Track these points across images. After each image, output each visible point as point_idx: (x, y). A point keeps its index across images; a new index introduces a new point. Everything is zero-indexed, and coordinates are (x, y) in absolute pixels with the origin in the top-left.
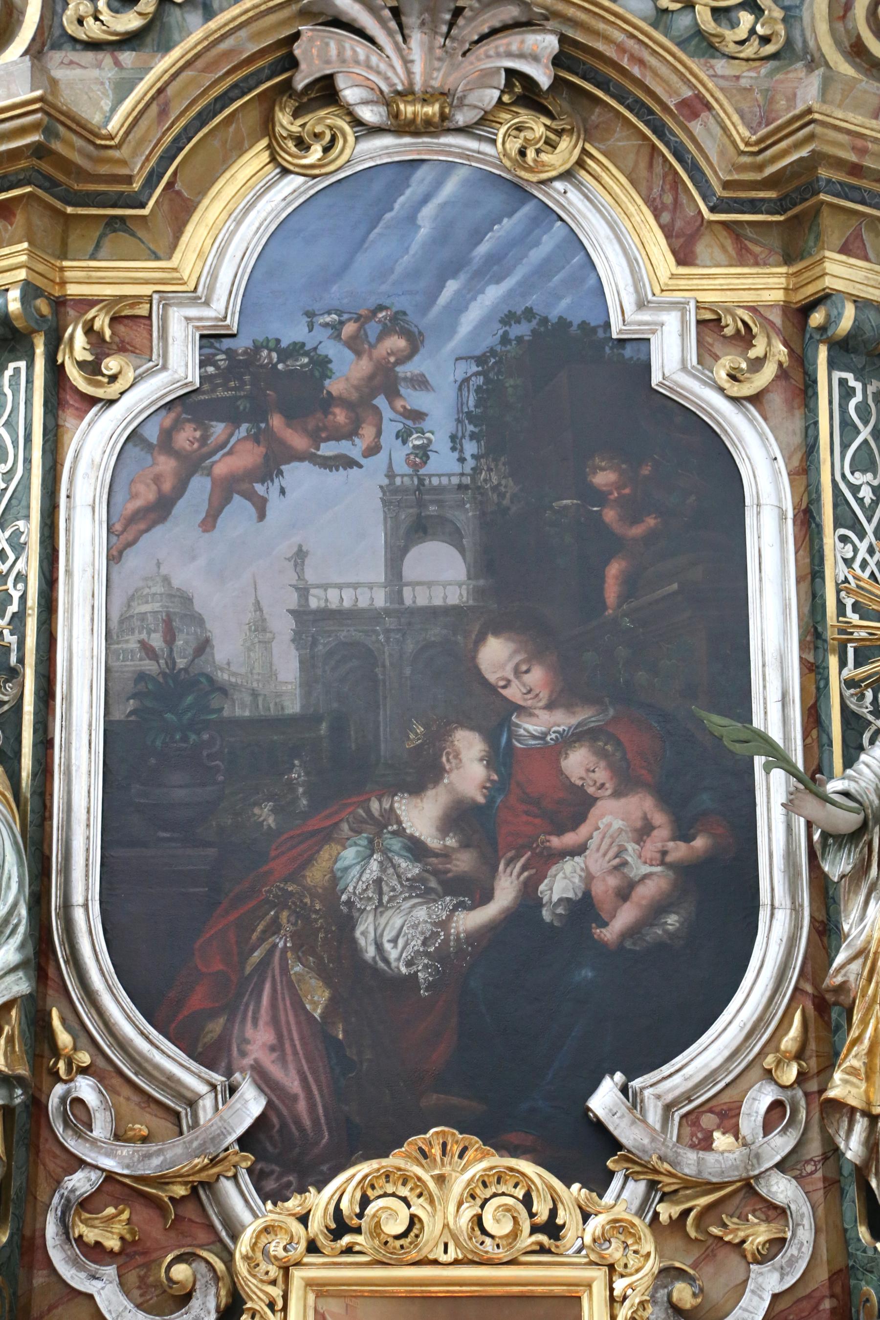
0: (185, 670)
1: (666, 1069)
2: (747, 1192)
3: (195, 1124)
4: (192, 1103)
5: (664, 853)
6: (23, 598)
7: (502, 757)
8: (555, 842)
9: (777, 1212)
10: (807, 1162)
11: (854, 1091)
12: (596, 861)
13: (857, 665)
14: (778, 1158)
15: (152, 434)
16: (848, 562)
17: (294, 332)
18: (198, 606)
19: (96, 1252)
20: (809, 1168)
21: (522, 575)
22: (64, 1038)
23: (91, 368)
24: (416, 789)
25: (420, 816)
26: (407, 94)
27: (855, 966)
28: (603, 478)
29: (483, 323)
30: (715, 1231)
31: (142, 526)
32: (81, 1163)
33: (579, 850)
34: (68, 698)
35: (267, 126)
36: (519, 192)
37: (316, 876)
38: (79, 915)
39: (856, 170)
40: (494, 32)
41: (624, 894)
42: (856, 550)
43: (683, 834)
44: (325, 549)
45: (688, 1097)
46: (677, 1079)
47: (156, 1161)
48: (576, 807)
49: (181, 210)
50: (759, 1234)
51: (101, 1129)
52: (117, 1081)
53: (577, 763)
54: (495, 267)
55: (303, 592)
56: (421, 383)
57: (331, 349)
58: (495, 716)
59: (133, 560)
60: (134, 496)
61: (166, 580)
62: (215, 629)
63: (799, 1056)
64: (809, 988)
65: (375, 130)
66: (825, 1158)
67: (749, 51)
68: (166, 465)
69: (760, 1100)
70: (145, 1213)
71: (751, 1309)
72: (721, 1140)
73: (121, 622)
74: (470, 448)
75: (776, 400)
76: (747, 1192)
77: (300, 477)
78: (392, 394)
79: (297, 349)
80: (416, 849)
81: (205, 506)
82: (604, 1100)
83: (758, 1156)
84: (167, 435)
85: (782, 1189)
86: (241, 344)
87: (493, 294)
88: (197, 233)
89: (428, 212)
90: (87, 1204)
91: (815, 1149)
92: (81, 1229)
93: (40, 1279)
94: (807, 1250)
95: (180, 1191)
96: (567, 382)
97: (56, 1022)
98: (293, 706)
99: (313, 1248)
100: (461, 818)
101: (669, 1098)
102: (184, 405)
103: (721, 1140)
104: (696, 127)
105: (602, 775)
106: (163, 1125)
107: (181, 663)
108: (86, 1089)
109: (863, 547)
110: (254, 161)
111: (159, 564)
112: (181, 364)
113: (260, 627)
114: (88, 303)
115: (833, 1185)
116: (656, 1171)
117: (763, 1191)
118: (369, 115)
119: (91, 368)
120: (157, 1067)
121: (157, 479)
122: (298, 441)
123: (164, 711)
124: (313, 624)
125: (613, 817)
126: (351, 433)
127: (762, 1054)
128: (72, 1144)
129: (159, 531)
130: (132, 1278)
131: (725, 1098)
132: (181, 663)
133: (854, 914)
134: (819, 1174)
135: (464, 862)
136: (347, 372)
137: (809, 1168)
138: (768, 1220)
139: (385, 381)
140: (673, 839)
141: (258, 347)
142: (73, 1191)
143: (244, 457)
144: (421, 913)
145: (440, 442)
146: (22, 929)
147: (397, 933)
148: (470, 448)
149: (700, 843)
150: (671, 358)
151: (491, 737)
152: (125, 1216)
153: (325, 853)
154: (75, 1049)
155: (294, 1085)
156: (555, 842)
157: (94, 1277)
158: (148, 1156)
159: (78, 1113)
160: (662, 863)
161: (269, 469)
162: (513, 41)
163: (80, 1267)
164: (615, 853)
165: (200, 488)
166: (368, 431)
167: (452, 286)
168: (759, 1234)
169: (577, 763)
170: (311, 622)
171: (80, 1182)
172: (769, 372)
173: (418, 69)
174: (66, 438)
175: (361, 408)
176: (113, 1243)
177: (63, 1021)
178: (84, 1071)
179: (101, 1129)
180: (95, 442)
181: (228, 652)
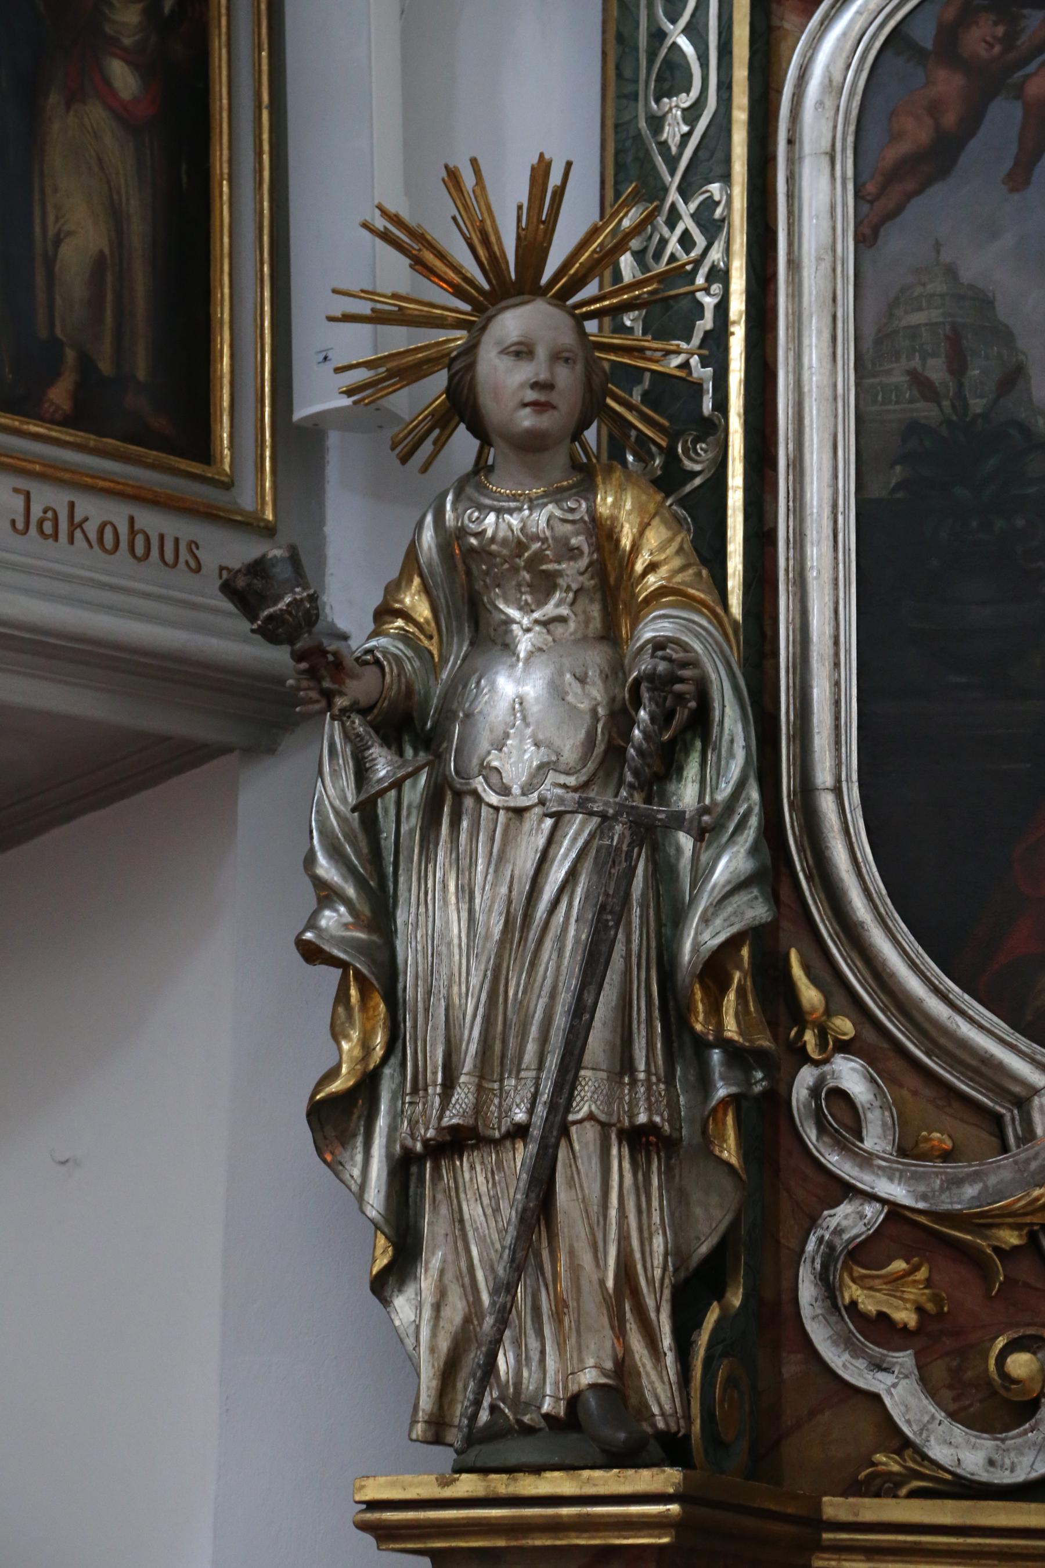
0: (985, 416)
3: (1028, 1135)
6: (722, 308)
15: (925, 35)
18: (1002, 312)
19: (879, 1330)
22: (810, 995)
31: (910, 185)
32: (847, 1191)
34: (797, 465)
38: (827, 804)
47: (970, 1191)
51: (875, 1139)
52: (896, 1065)
59: (896, 242)
60: (895, 137)
61: (951, 272)
68: (948, 84)
73: (878, 342)
81: (1014, 149)
90: (863, 1254)
92: (853, 1292)
93: (792, 1367)
95: (1012, 1238)
97: (797, 971)
106: (976, 1136)
107: (977, 405)
108: (850, 1075)
111: (937, 247)
120: (964, 1044)
121: (934, 109)
128: (833, 1160)
129: (937, 192)
130: (939, 1370)
132: (977, 405)
142: (838, 1231)
146: (754, 821)
152: (922, 1274)
154: (828, 1013)
157: (878, 1366)
158: (958, 1182)
159: (839, 1113)
163: (856, 1352)
165: (1004, 118)
171: (849, 1220)
174: (784, 47)
176: (905, 1316)
177: (807, 968)
178: (844, 1047)
179: (875, 1139)
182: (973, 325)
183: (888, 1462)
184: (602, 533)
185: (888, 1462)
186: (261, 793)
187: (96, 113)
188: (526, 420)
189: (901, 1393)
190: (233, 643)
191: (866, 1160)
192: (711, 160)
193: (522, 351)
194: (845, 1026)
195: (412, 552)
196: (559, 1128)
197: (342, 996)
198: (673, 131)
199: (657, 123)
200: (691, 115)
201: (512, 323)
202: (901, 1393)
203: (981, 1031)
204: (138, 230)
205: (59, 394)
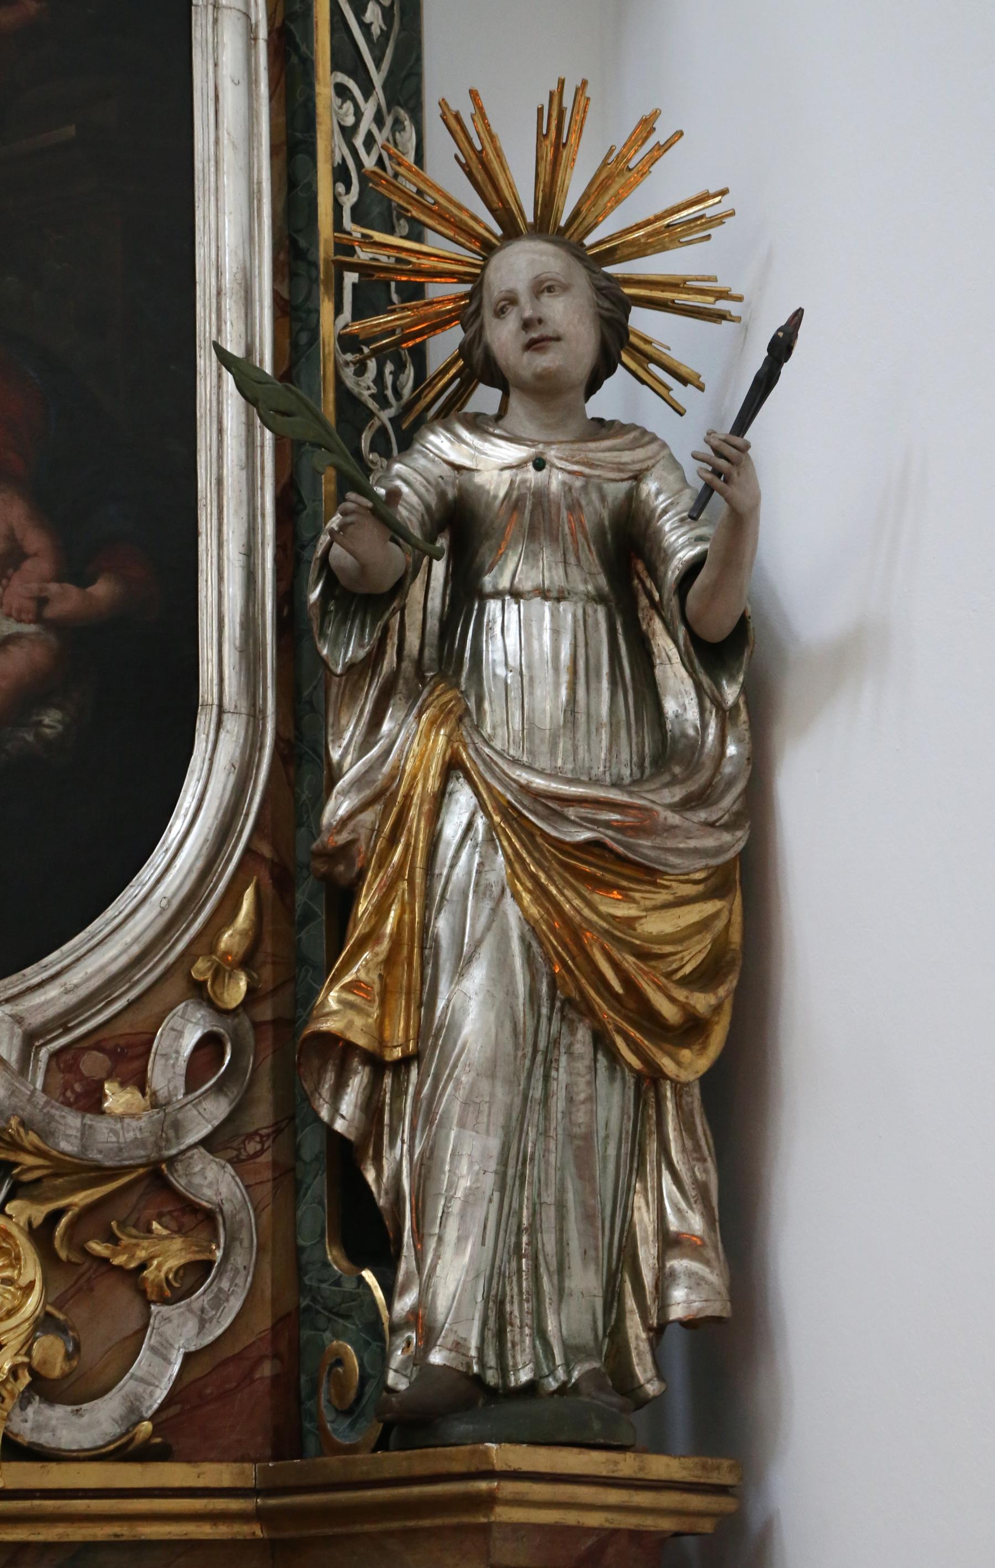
1: (33, 974)
2: (155, 1184)
5: (42, 601)
9: (198, 1218)
10: (250, 1137)
11: (359, 1021)
13: (357, 316)
14: (205, 1130)
16: (348, 133)
20: (252, 1147)
27: (368, 817)
30: (97, 1247)
42: (358, 114)
43: (75, 571)
45: (63, 1022)
46: (52, 992)
63: (247, 962)
64: (265, 850)
66: (277, 1131)
69: (186, 1032)
71: (150, 1378)
72: (117, 1098)
76: (155, 1184)
83: (177, 1126)
85: (214, 1182)
91: (262, 1115)
94: (244, 1283)
101: (35, 1020)
103: (117, 1098)
109: (369, 110)
115: (288, 1178)
116: (16, 1146)
117: (179, 1183)
127: (188, 956)
131: (123, 1027)
134: (266, 1158)
137: (252, 1147)
138: (180, 1231)
140: (58, 579)
149: (102, 589)
160: (38, 619)
168: (167, 1255)
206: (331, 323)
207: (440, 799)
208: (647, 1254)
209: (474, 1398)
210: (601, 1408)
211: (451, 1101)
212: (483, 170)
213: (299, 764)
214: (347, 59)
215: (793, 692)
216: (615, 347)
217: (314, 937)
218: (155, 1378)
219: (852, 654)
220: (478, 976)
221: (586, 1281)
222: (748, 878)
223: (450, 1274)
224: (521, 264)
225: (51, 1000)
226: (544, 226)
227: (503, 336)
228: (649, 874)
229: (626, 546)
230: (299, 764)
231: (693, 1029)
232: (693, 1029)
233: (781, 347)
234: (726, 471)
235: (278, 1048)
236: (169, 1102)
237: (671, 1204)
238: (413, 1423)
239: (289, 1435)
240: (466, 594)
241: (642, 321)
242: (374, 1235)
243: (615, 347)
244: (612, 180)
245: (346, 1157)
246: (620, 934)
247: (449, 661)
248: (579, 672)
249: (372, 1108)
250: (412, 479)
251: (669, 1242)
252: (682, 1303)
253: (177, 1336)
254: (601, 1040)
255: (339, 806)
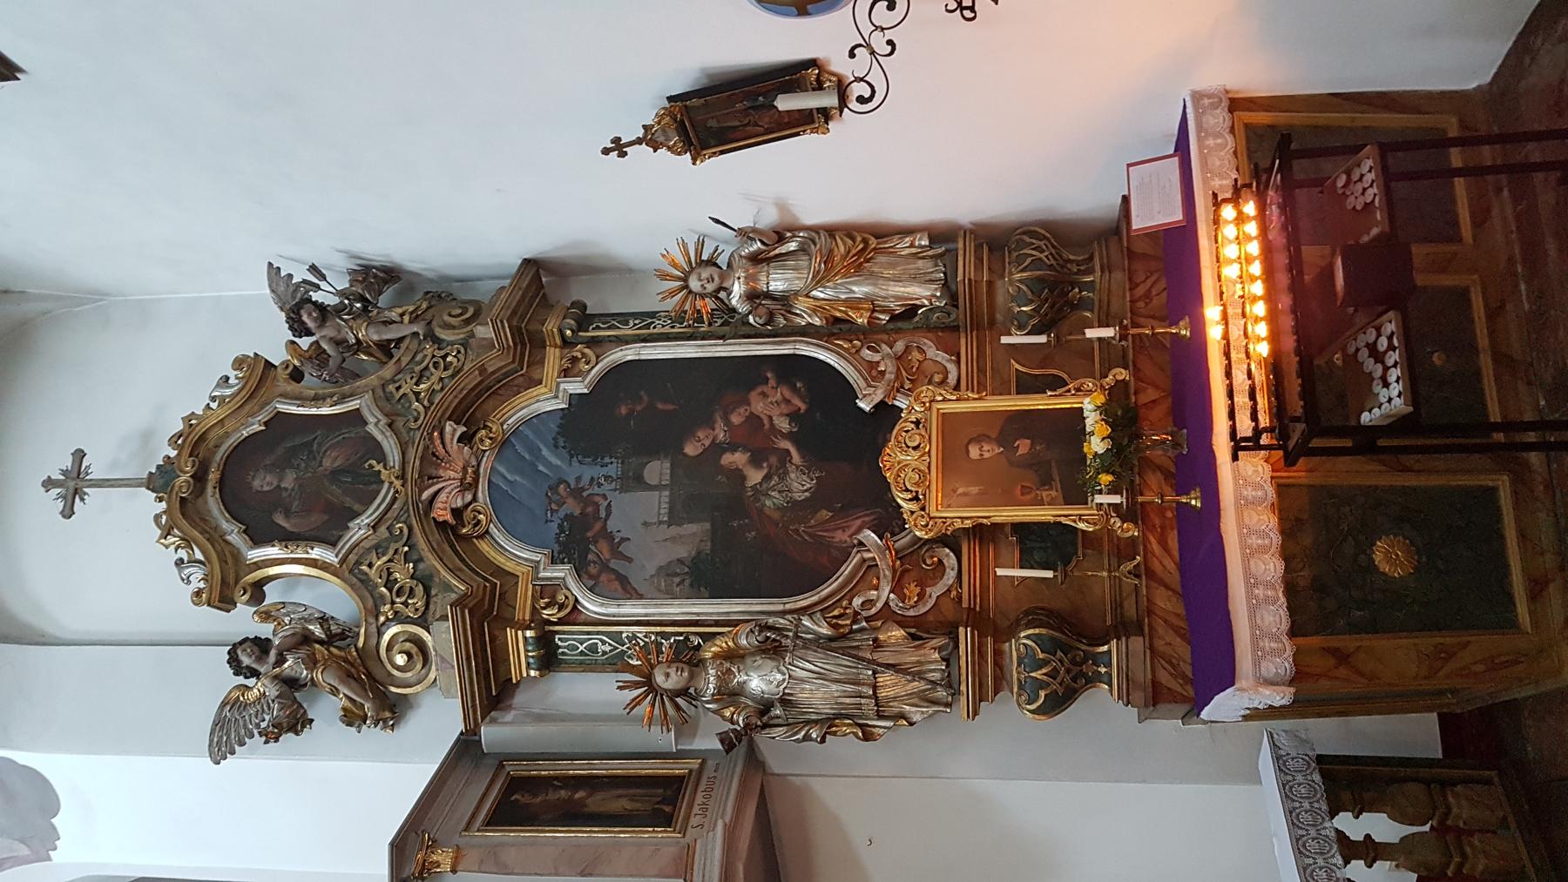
4: (864, 560)
6: (657, 634)
7: (733, 448)
8: (767, 426)
9: (907, 349)
12: (775, 412)
15: (592, 583)
17: (554, 526)
19: (921, 596)
21: (660, 438)
22: (836, 613)
23: (561, 607)
24: (744, 478)
25: (755, 477)
26: (462, 480)
28: (624, 410)
29: (557, 456)
32: (887, 603)
33: (770, 418)
34: (698, 614)
35: (467, 539)
36: (505, 443)
37: (776, 515)
38: (788, 606)
39: (514, 313)
40: (443, 443)
41: (787, 402)
44: (643, 516)
48: (754, 419)
49: (500, 572)
50: (916, 355)
53: (736, 419)
54: (535, 452)
55: (661, 522)
56: (578, 479)
57: (562, 514)
58: (717, 449)
62: (674, 557)
65: (475, 499)
67: (461, 357)
68: (603, 578)
69: (866, 353)
70: (906, 578)
74: (607, 460)
75: (598, 351)
77: (612, 525)
78: (583, 489)
79: (560, 526)
80: (767, 478)
82: (865, 406)
84: (591, 577)
85: (900, 346)
86: (556, 547)
87: (545, 452)
88: (509, 566)
89: (509, 477)
91: (885, 337)
93: (930, 618)
96: (581, 426)
98: (708, 525)
99: (923, 509)
100: (756, 462)
102: (580, 572)
104: (490, 370)
105: (742, 410)
108: (857, 602)
110: (483, 546)
112: (561, 572)
113: (673, 539)
114: (534, 608)
115: (898, 331)
118: (469, 497)
119: (561, 607)
122: (598, 526)
123: (705, 577)
124: (674, 519)
125: (758, 406)
126: (597, 505)
128: (879, 605)
133: (798, 320)
135: (773, 460)
136: (572, 507)
139: (577, 492)
141: (558, 542)
143: (603, 548)
144: (793, 476)
145: (604, 471)
147: (800, 485)
148: (607, 460)
150: (577, 387)
151: (724, 451)
153: (767, 511)
155: (858, 522)
156: (767, 426)
159: (869, 603)
161: (610, 537)
162: (448, 437)
164: (773, 406)
165: (613, 564)
166: (597, 499)
167: (541, 468)
168: (916, 355)
169: (736, 419)
170: (674, 519)
172: (587, 351)
173: (452, 474)
175: (588, 501)
176: (918, 590)
180: (592, 606)
181: (683, 552)
182: (666, 571)
183: (954, 593)
184: (716, 656)
185: (954, 593)
186: (775, 764)
187: (589, 801)
188: (686, 674)
189: (935, 591)
190: (741, 750)
191: (879, 597)
192: (617, 637)
193: (667, 675)
194: (845, 603)
195: (714, 712)
196: (873, 662)
197: (834, 734)
198: (608, 648)
199: (604, 653)
200: (604, 643)
201: (659, 679)
202: (935, 591)
203: (847, 569)
204: (620, 792)
205: (667, 809)
206: (705, 328)
207: (815, 298)
208: (914, 250)
209: (947, 286)
210: (948, 259)
211: (883, 293)
212: (672, 293)
213: (807, 332)
214: (647, 326)
215: (788, 221)
216: (711, 262)
217: (844, 327)
218: (941, 357)
219: (782, 207)
220: (855, 288)
221: (920, 263)
222: (831, 231)
223: (922, 293)
224: (694, 284)
225: (862, 383)
226: (685, 280)
227: (710, 287)
228: (831, 251)
229: (755, 259)
230: (807, 332)
231: (865, 241)
232: (865, 241)
233: (717, 221)
234: (745, 234)
235: (870, 334)
236: (883, 357)
237: (903, 246)
238: (953, 298)
239: (955, 329)
240: (768, 295)
241: (705, 257)
242: (911, 311)
243: (711, 262)
244: (675, 265)
245: (894, 318)
246: (844, 258)
247: (784, 301)
248: (784, 268)
249: (883, 312)
250: (743, 308)
251: (912, 246)
252: (925, 242)
253: (933, 352)
254: (868, 261)
255: (817, 321)
